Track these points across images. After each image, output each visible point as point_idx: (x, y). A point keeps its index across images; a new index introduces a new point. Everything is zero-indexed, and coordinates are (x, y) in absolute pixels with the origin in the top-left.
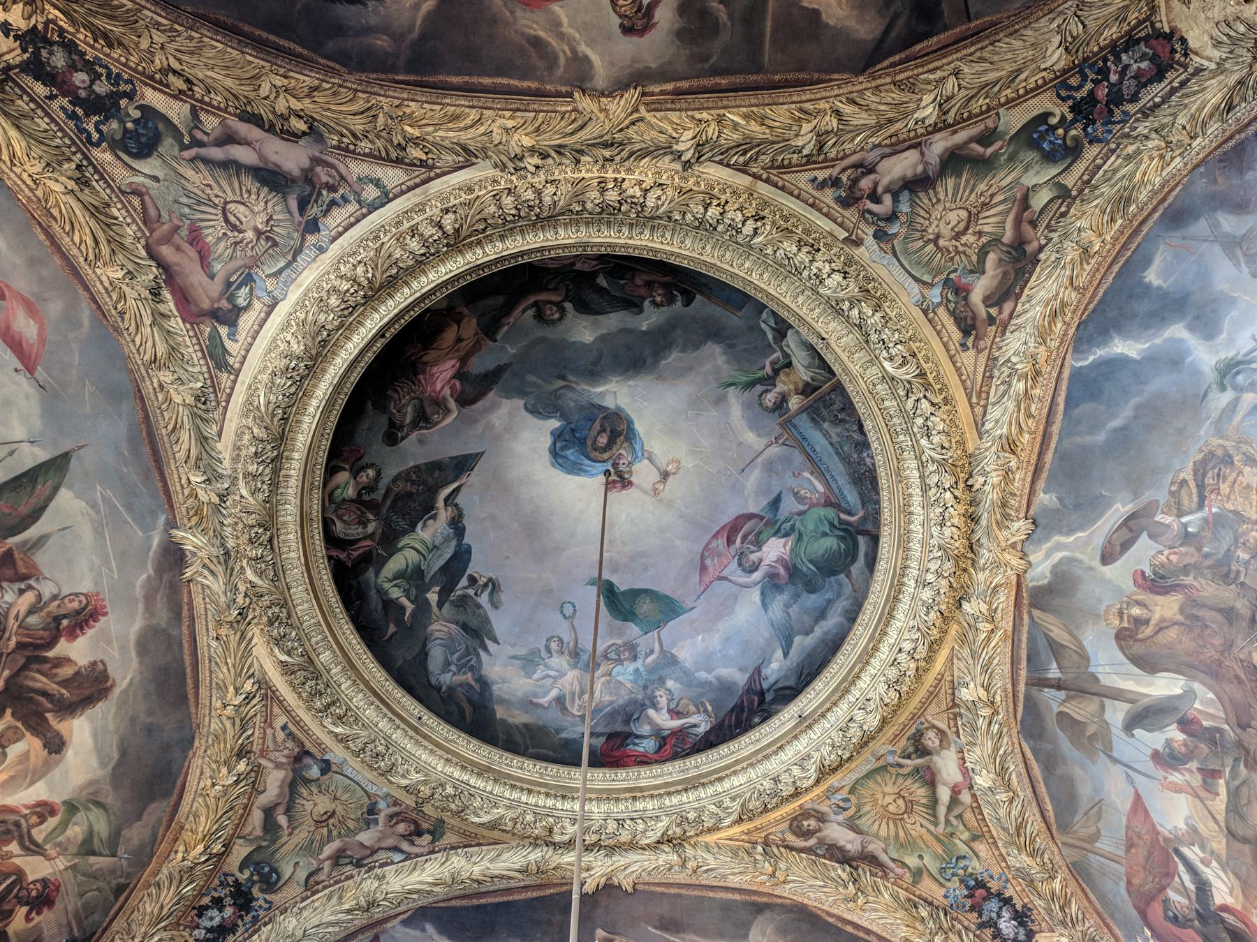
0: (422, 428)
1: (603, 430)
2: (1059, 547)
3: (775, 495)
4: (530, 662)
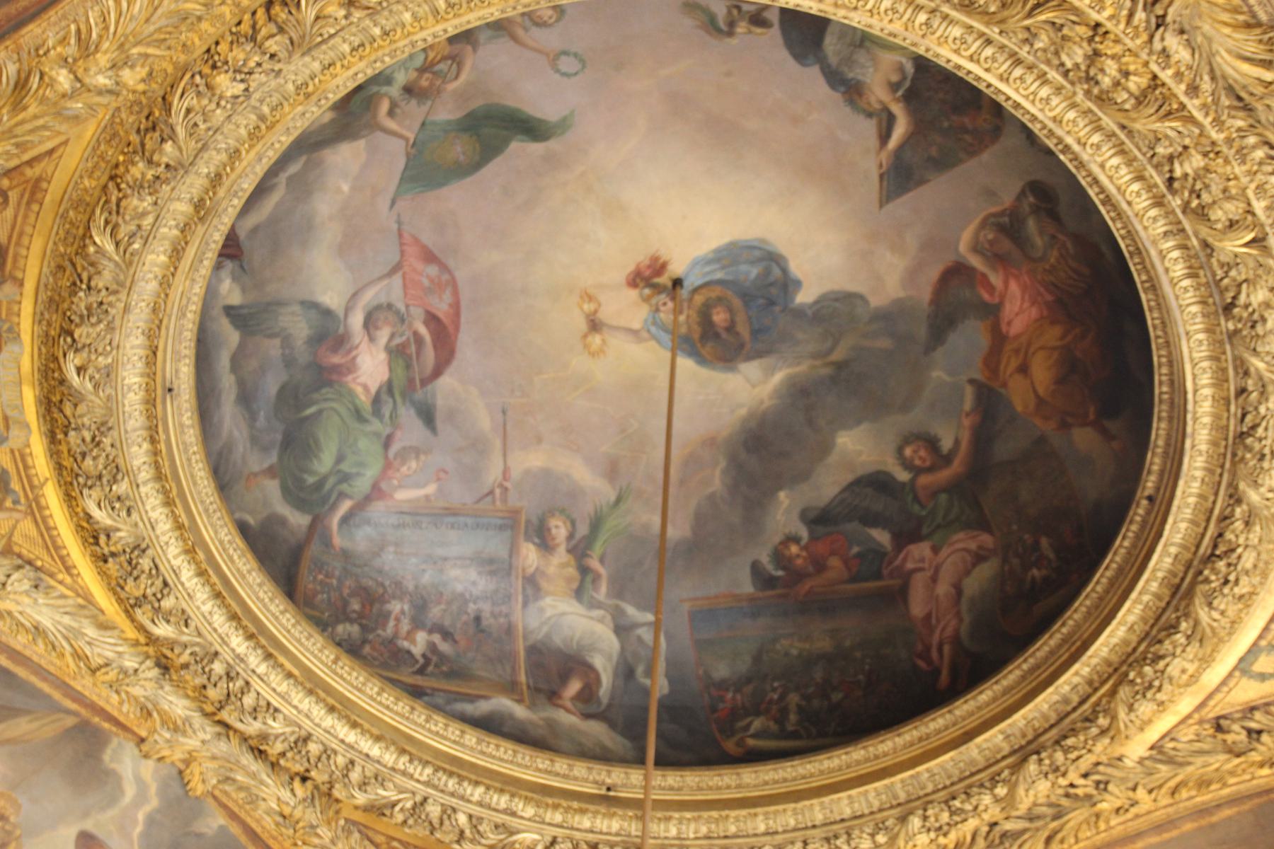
0: (1002, 213)
1: (731, 328)
2: (141, 797)
3: (439, 424)
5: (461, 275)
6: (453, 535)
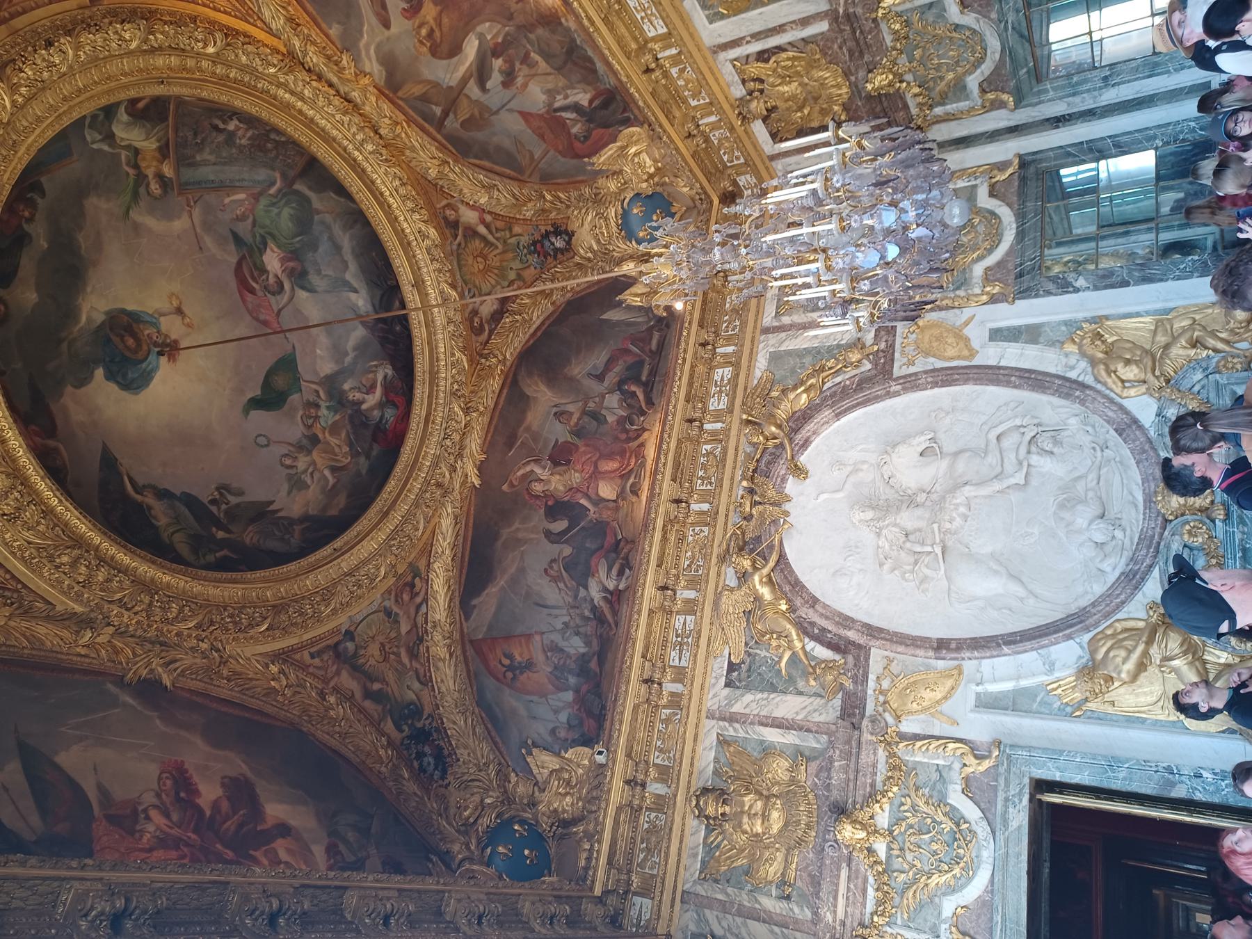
1: (122, 337)
4: (296, 484)
5: (248, 318)
6: (212, 177)
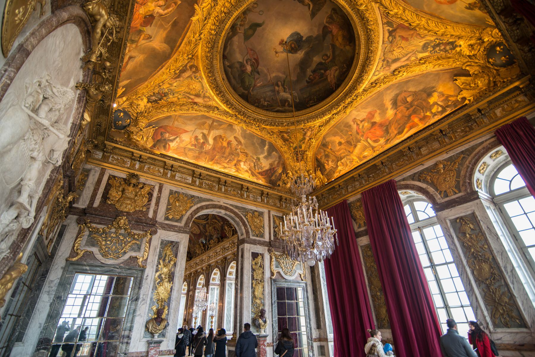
2: (239, 131)
